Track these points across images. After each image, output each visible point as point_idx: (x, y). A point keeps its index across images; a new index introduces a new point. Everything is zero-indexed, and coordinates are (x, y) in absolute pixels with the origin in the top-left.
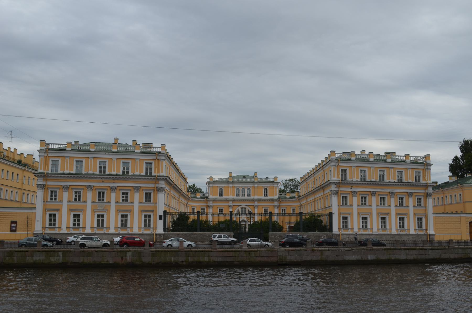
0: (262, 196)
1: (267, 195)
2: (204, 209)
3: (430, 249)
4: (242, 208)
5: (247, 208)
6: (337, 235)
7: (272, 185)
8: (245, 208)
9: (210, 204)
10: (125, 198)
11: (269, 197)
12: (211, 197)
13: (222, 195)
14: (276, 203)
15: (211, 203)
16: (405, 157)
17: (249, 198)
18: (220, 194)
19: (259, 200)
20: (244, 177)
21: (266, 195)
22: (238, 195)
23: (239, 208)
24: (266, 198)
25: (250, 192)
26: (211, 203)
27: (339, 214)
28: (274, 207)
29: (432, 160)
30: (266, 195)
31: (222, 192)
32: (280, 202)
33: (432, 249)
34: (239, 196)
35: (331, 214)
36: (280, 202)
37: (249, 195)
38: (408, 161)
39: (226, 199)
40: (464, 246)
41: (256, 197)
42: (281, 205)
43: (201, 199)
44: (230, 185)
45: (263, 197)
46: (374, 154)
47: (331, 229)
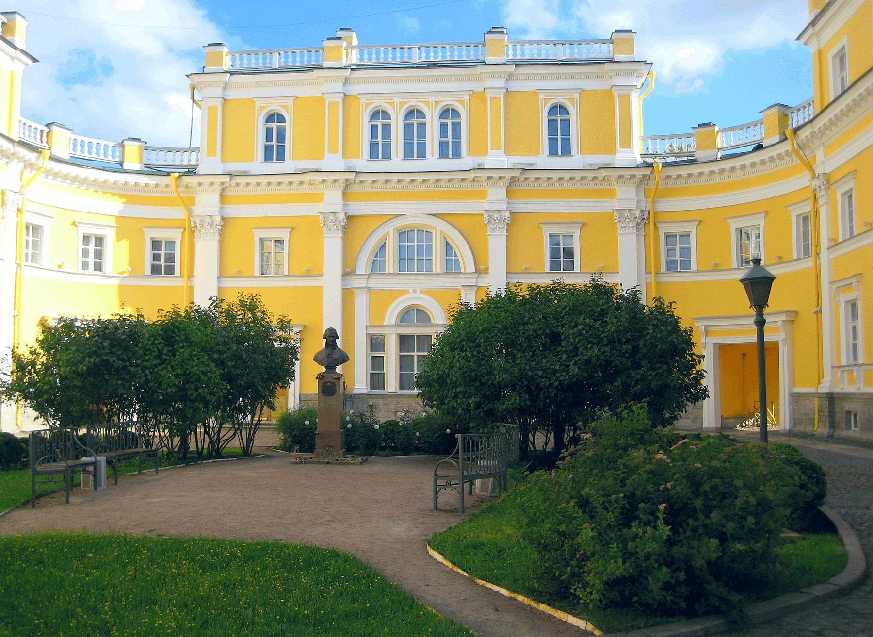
0: (537, 152)
4: (402, 233)
11: (577, 160)
21: (559, 143)
23: (390, 231)
30: (559, 143)
31: (281, 137)
41: (497, 159)
42: (666, 205)
43: (143, 180)
45: (543, 160)
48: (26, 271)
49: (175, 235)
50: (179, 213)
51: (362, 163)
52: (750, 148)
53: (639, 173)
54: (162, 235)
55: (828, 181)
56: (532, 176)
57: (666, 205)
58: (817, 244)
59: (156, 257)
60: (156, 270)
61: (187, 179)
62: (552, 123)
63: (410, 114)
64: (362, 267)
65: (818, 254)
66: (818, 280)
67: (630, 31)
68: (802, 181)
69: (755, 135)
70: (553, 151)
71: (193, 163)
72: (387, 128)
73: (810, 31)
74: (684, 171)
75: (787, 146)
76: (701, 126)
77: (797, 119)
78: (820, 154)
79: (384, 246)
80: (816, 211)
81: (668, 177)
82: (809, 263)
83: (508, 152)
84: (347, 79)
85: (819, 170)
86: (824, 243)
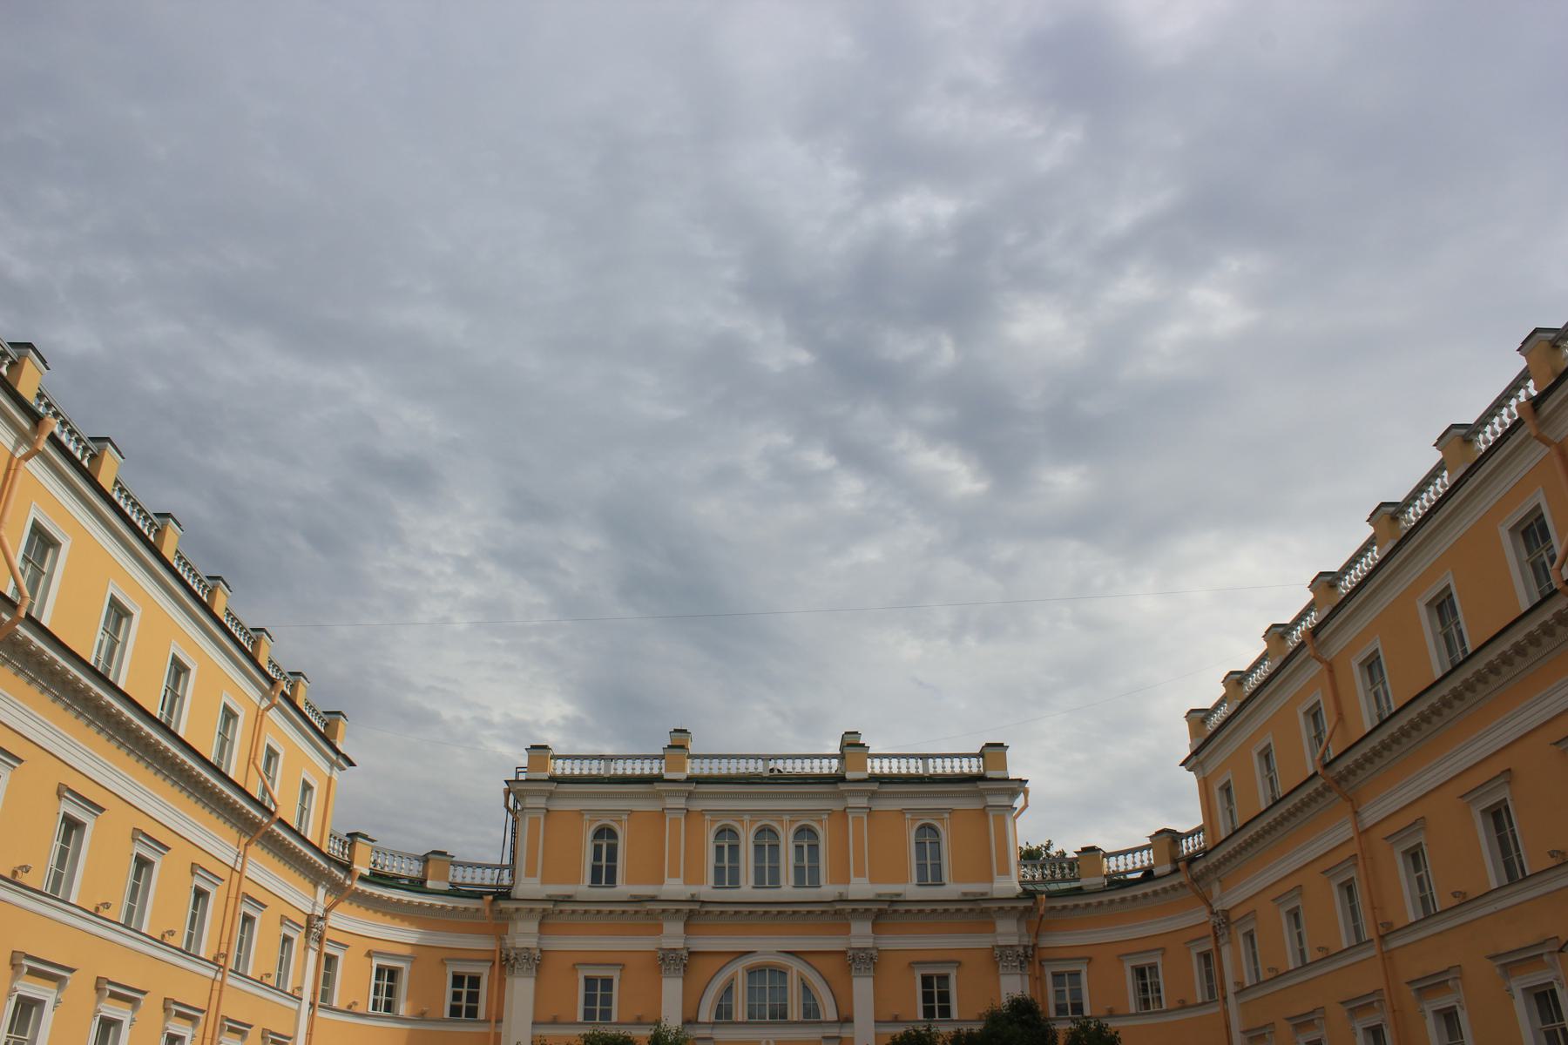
4: (752, 972)
7: (973, 804)
8: (780, 973)
9: (521, 942)
12: (529, 886)
13: (611, 880)
14: (1008, 932)
15: (524, 935)
19: (884, 912)
22: (726, 875)
23: (739, 969)
26: (524, 935)
28: (999, 957)
30: (931, 874)
37: (806, 874)
39: (637, 900)
41: (861, 887)
43: (449, 903)
44: (671, 803)
45: (910, 889)
48: (320, 1014)
49: (483, 971)
51: (706, 890)
52: (1139, 875)
53: (1021, 905)
55: (1227, 918)
56: (902, 908)
58: (1223, 988)
59: (457, 996)
60: (455, 1011)
61: (503, 905)
62: (920, 845)
63: (762, 832)
64: (706, 1014)
65: (1225, 998)
66: (1228, 1027)
67: (1001, 745)
68: (1201, 915)
69: (1146, 858)
70: (922, 882)
71: (506, 882)
72: (734, 849)
73: (1194, 760)
74: (1070, 902)
75: (1181, 878)
76: (1085, 850)
77: (1188, 846)
78: (1216, 889)
79: (730, 988)
80: (1218, 950)
81: (1053, 908)
82: (1217, 1009)
83: (872, 881)
84: (690, 793)
85: (1217, 907)
86: (1230, 988)
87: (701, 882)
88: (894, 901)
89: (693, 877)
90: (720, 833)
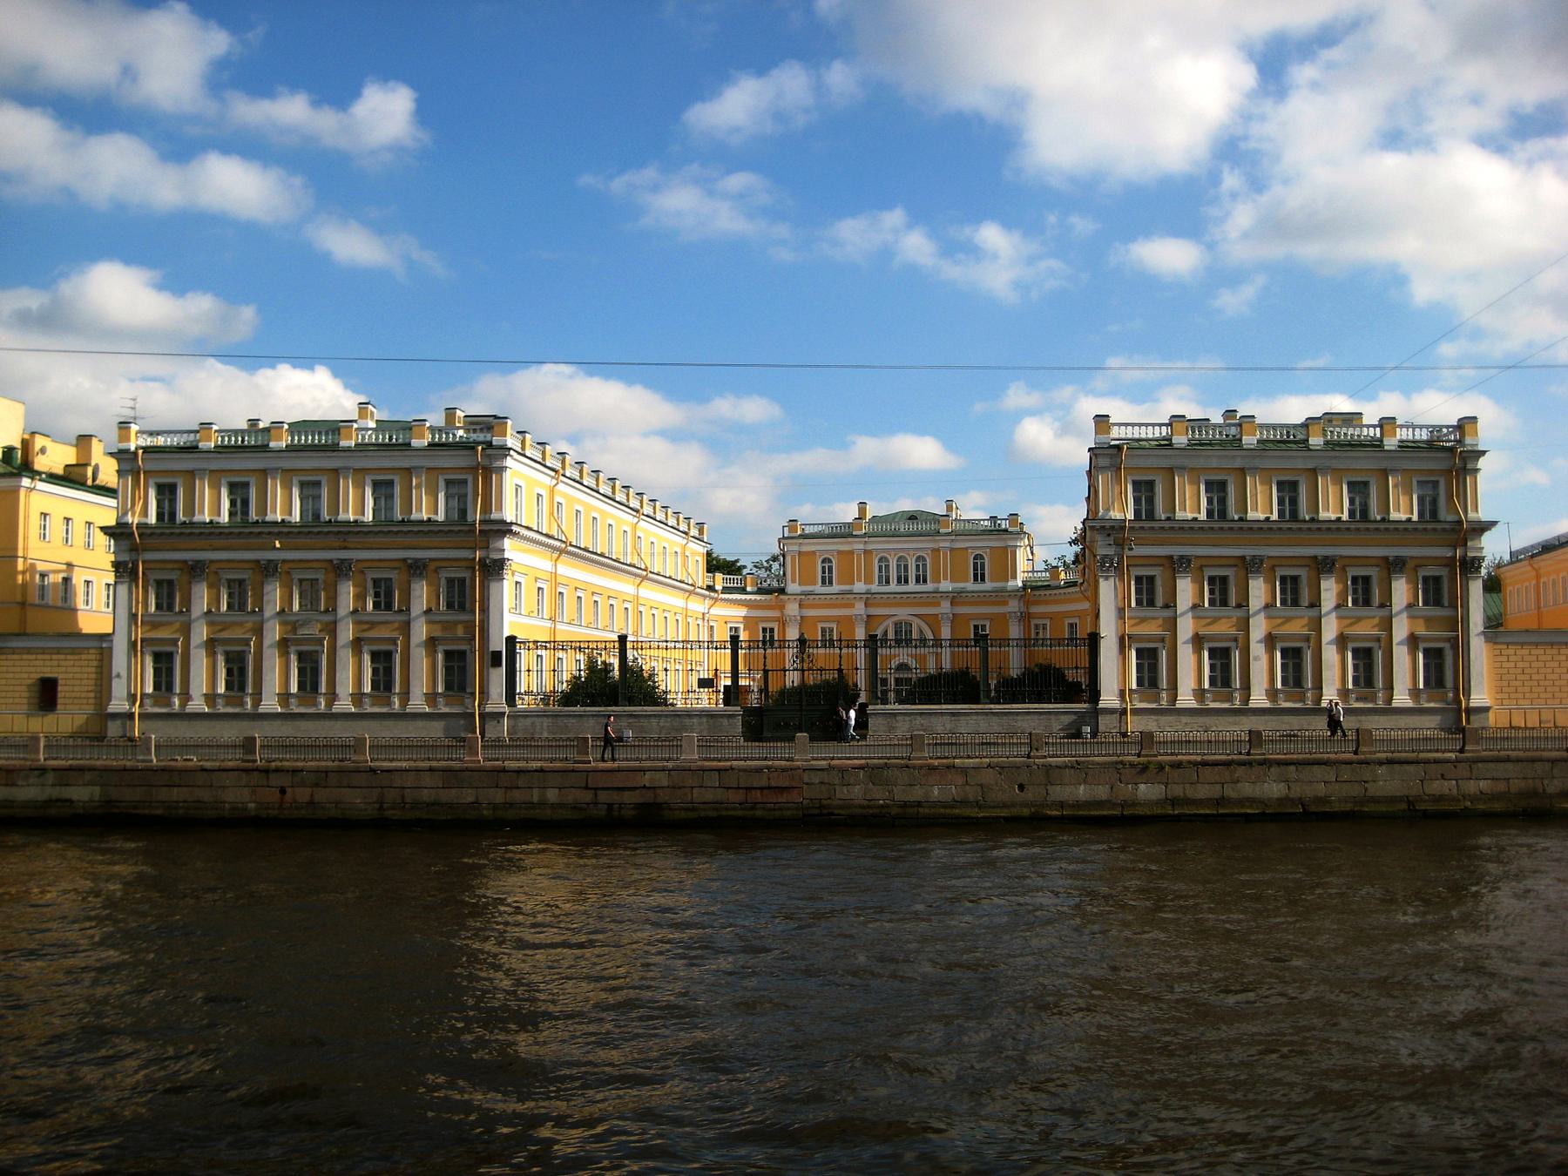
0: (967, 581)
1: (983, 579)
2: (772, 630)
3: (1381, 763)
5: (916, 622)
6: (1111, 711)
10: (382, 598)
13: (831, 583)
16: (1381, 426)
17: (921, 588)
18: (975, 576)
20: (912, 517)
23: (890, 624)
24: (980, 587)
25: (925, 571)
27: (1122, 639)
29: (1484, 436)
30: (979, 577)
32: (1028, 604)
33: (1390, 762)
34: (888, 582)
35: (1094, 640)
36: (1028, 604)
38: (1390, 443)
40: (527, 760)
41: (946, 585)
42: (1034, 609)
43: (758, 597)
45: (970, 586)
46: (1258, 421)
47: (1095, 695)
50: (776, 614)
51: (875, 588)
54: (768, 625)
57: (1034, 609)
72: (887, 567)
87: (871, 582)
88: (960, 592)
89: (868, 581)
90: (880, 560)
